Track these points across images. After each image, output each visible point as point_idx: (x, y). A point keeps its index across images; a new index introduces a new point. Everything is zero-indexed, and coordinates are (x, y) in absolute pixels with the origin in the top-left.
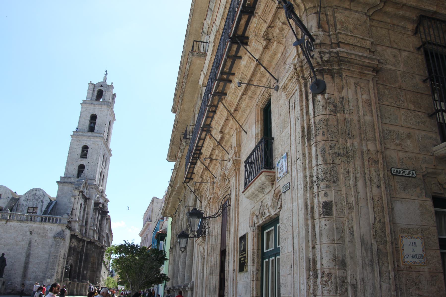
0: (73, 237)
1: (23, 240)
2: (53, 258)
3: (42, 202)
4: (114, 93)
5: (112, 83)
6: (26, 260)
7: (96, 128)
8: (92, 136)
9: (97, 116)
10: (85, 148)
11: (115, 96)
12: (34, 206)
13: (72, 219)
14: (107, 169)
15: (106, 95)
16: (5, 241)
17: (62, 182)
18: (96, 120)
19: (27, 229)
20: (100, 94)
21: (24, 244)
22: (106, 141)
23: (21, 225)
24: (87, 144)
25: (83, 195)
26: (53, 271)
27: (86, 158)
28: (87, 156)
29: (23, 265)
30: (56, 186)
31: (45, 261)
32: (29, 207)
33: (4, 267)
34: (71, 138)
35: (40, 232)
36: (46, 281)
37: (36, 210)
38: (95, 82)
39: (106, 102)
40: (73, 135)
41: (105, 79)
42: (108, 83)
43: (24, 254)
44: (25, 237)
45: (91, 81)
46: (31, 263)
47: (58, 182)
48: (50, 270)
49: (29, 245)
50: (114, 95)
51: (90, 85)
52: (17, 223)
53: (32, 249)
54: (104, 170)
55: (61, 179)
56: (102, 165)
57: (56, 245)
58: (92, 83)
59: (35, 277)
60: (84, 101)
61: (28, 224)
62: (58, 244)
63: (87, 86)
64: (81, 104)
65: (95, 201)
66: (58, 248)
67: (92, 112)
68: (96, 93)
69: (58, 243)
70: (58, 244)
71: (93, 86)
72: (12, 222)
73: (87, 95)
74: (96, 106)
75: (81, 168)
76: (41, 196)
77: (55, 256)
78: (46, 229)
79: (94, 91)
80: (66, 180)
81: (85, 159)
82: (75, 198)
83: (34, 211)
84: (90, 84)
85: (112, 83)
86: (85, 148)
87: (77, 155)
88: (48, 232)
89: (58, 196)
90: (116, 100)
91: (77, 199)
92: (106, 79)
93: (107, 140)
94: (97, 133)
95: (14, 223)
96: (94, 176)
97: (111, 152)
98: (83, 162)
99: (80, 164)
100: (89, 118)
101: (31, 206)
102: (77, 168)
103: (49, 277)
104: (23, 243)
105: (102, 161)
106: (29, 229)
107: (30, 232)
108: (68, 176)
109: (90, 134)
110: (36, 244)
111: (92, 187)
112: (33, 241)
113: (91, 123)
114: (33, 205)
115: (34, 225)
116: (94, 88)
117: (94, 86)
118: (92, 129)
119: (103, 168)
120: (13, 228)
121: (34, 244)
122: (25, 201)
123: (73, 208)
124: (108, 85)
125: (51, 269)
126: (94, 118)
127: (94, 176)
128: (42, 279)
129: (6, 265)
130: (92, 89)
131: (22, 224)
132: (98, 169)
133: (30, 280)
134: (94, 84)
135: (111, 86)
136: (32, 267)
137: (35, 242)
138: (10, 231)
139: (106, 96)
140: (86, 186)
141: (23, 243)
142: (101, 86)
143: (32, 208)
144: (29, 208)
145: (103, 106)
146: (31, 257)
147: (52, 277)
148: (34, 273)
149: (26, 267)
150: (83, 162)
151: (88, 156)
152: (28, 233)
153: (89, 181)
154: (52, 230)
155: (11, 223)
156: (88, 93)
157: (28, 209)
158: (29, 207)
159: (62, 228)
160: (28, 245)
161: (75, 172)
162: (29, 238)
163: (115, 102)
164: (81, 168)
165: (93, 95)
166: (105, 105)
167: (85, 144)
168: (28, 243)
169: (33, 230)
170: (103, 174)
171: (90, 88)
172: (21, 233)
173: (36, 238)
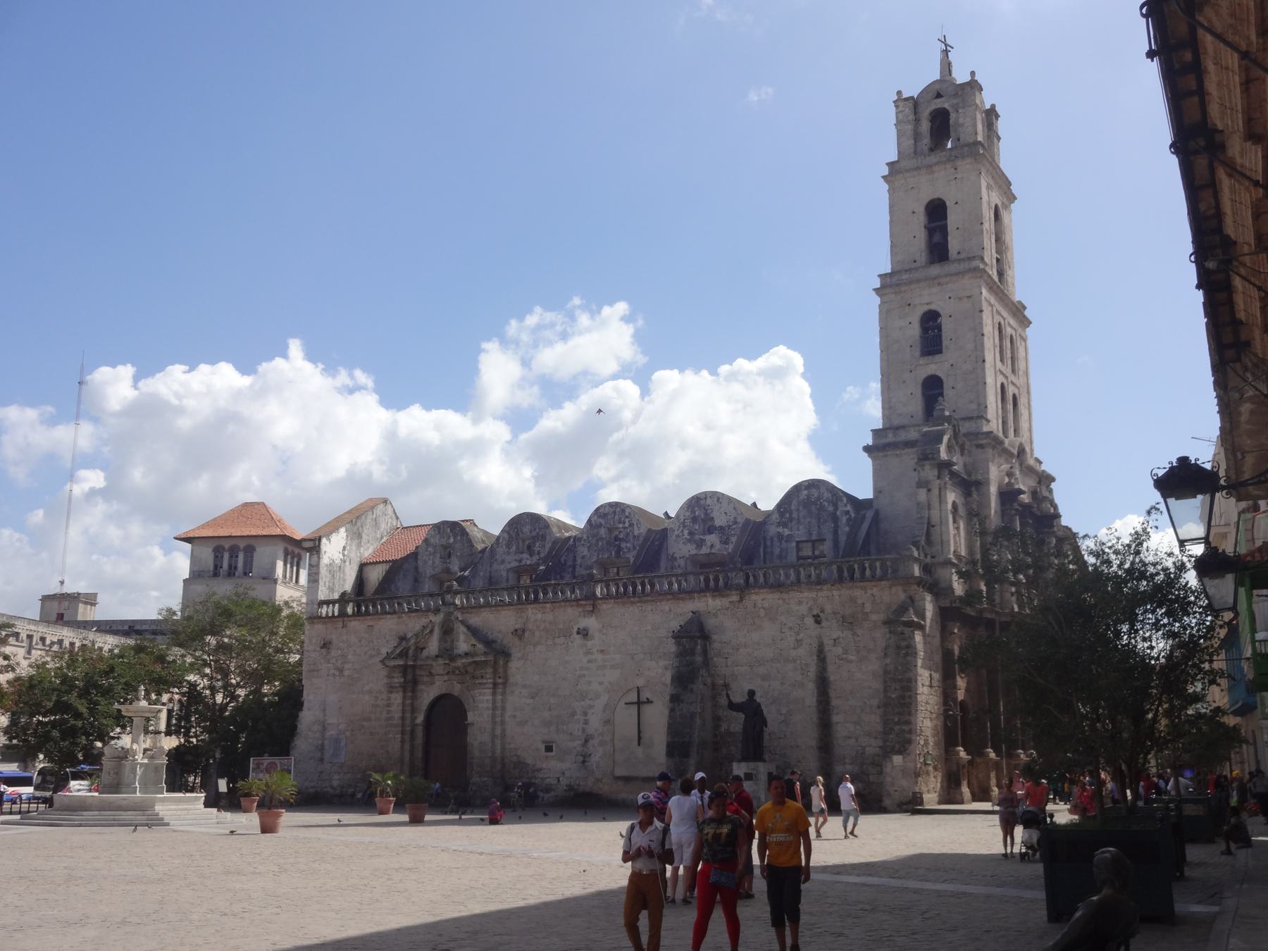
0: (946, 615)
1: (799, 642)
2: (898, 687)
3: (835, 519)
4: (988, 107)
5: (973, 73)
6: (819, 702)
7: (954, 244)
8: (946, 276)
9: (948, 204)
10: (931, 320)
11: (997, 116)
12: (814, 538)
13: (933, 557)
14: (1021, 373)
15: (961, 121)
17: (880, 447)
18: (946, 218)
19: (803, 609)
20: (941, 125)
21: (805, 654)
22: (995, 278)
24: (933, 307)
25: (953, 475)
26: (904, 727)
27: (940, 352)
28: (940, 343)
30: (867, 463)
31: (875, 702)
32: (798, 542)
33: (762, 731)
34: (877, 300)
36: (891, 761)
37: (821, 548)
38: (913, 90)
39: (968, 145)
40: (883, 286)
41: (947, 66)
42: (960, 76)
43: (811, 687)
44: (802, 635)
45: (899, 93)
47: (867, 449)
48: (897, 728)
49: (818, 656)
50: (992, 114)
51: (901, 104)
52: (770, 596)
54: (1012, 378)
55: (874, 438)
56: (1002, 360)
57: (898, 647)
58: (905, 95)
60: (891, 165)
61: (801, 595)
62: (904, 644)
63: (892, 110)
64: (884, 177)
65: (999, 487)
66: (907, 654)
67: (927, 195)
68: (925, 126)
69: (904, 639)
71: (909, 107)
72: (756, 594)
73: (899, 144)
74: (935, 168)
75: (933, 388)
76: (826, 504)
78: (860, 601)
79: (917, 121)
80: (890, 438)
81: (937, 357)
82: (929, 490)
83: (817, 553)
84: (900, 101)
85: (973, 73)
86: (931, 320)
87: (908, 349)
89: (877, 491)
90: (1002, 126)
91: (935, 491)
92: (950, 64)
93: (1001, 274)
94: (960, 260)
96: (979, 405)
97: (1027, 313)
98: (933, 367)
99: (925, 376)
100: (921, 218)
101: (804, 539)
102: (918, 391)
103: (897, 746)
104: (801, 651)
105: (998, 350)
106: (810, 609)
107: (814, 616)
108: (896, 422)
109: (935, 270)
110: (839, 650)
111: (981, 442)
112: (828, 643)
113: (930, 231)
114: (811, 534)
115: (820, 594)
116: (915, 113)
117: (915, 103)
118: (938, 251)
119: (1008, 371)
121: (833, 652)
122: (785, 525)
123: (929, 523)
124: (963, 86)
125: (898, 723)
126: (936, 211)
127: (979, 405)
128: (878, 755)
129: (765, 723)
130: (912, 117)
131: (785, 596)
132: (990, 380)
133: (844, 764)
134: (912, 98)
135: (973, 86)
136: (843, 727)
137: (834, 646)
139: (962, 125)
140: (957, 443)
142: (939, 96)
143: (810, 544)
144: (801, 545)
145: (959, 163)
146: (832, 694)
147: (905, 750)
148: (853, 741)
149: (825, 724)
150: (933, 367)
151: (944, 344)
152: (810, 621)
153: (965, 427)
155: (754, 597)
156: (900, 135)
157: (798, 549)
158: (798, 542)
159: (905, 591)
160: (815, 658)
161: (916, 406)
163: (999, 138)
164: (933, 388)
165: (917, 136)
166: (963, 157)
167: (926, 308)
168: (815, 651)
169: (822, 611)
170: (1011, 394)
171: (900, 116)
173: (835, 636)
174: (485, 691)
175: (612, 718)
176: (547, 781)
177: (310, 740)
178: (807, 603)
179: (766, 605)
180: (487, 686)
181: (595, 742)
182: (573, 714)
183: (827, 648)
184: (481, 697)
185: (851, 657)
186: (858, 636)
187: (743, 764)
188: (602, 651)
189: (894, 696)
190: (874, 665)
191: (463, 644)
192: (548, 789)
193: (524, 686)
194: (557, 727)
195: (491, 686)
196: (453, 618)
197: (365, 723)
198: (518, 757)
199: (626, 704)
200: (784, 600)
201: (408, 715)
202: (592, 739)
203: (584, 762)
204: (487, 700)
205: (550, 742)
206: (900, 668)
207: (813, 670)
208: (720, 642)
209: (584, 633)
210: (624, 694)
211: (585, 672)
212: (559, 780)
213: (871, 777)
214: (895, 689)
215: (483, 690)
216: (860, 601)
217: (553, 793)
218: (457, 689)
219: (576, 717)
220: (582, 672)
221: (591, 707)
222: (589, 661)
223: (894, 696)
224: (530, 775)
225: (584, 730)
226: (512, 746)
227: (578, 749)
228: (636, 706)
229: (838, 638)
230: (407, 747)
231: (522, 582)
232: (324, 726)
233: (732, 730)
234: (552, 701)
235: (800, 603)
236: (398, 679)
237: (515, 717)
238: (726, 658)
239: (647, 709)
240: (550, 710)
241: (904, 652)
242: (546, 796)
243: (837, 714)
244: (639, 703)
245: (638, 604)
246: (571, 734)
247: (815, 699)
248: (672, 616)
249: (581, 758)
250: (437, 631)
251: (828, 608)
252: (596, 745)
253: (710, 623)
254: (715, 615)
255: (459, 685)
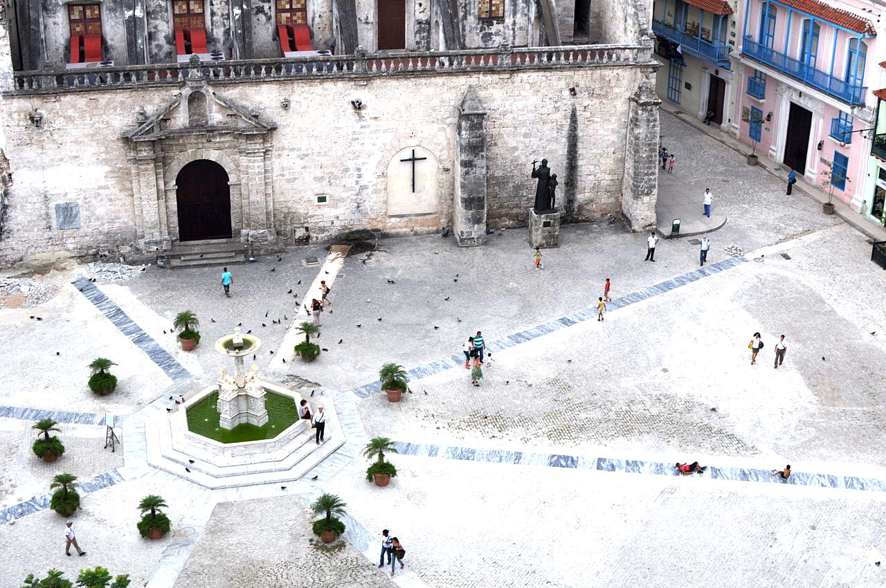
1: (557, 109)
2: (647, 149)
16: (514, 118)
19: (562, 84)
21: (561, 117)
23: (547, 77)
29: (565, 163)
35: (593, 87)
43: (564, 140)
46: (581, 157)
49: (571, 119)
53: (580, 126)
57: (648, 121)
59: (595, 184)
62: (652, 119)
70: (652, 119)
72: (524, 72)
77: (650, 145)
78: (607, 79)
88: (613, 84)
95: (529, 74)
103: (646, 190)
104: (558, 116)
106: (568, 84)
110: (588, 114)
120: (528, 86)
131: (548, 74)
136: (585, 165)
137: (585, 111)
138: (523, 93)
141: (558, 116)
146: (579, 145)
147: (651, 192)
148: (591, 177)
152: (566, 93)
154: (621, 79)
160: (569, 120)
162: (569, 103)
168: (569, 115)
172: (550, 96)
174: (256, 158)
175: (386, 171)
176: (321, 224)
177: (29, 211)
178: (566, 80)
179: (531, 81)
180: (256, 155)
181: (369, 191)
182: (347, 170)
183: (578, 113)
184: (251, 164)
185: (596, 119)
186: (603, 104)
187: (543, 216)
188: (376, 118)
189: (644, 156)
190: (614, 124)
191: (216, 117)
192: (323, 230)
193: (293, 149)
194: (329, 181)
195: (262, 154)
196: (203, 91)
197: (100, 191)
198: (289, 208)
199: (401, 161)
200: (547, 77)
201: (161, 183)
202: (367, 188)
203: (358, 207)
204: (258, 167)
205: (323, 194)
206: (649, 136)
207: (566, 128)
208: (490, 109)
209: (358, 106)
210: (397, 152)
211: (357, 136)
212: (333, 223)
213: (603, 200)
214: (646, 151)
215: (253, 158)
216: (607, 79)
217: (326, 234)
218: (213, 155)
219: (349, 173)
220: (354, 136)
221: (363, 163)
222: (362, 127)
223: (644, 156)
224: (302, 221)
225: (357, 183)
226: (282, 199)
227: (352, 197)
228: (411, 163)
229: (588, 105)
230: (163, 210)
231: (176, 8)
232: (46, 197)
233: (496, 175)
234: (324, 160)
235: (559, 79)
236: (145, 153)
237: (283, 175)
238: (494, 122)
239: (417, 163)
240: (321, 167)
241: (652, 124)
242: (320, 236)
243: (582, 159)
244: (413, 160)
245: (412, 79)
246: (344, 186)
247: (566, 150)
248: (446, 89)
249: (356, 205)
250: (184, 106)
251: (582, 84)
252: (370, 193)
253: (482, 94)
254: (486, 88)
255: (217, 152)
